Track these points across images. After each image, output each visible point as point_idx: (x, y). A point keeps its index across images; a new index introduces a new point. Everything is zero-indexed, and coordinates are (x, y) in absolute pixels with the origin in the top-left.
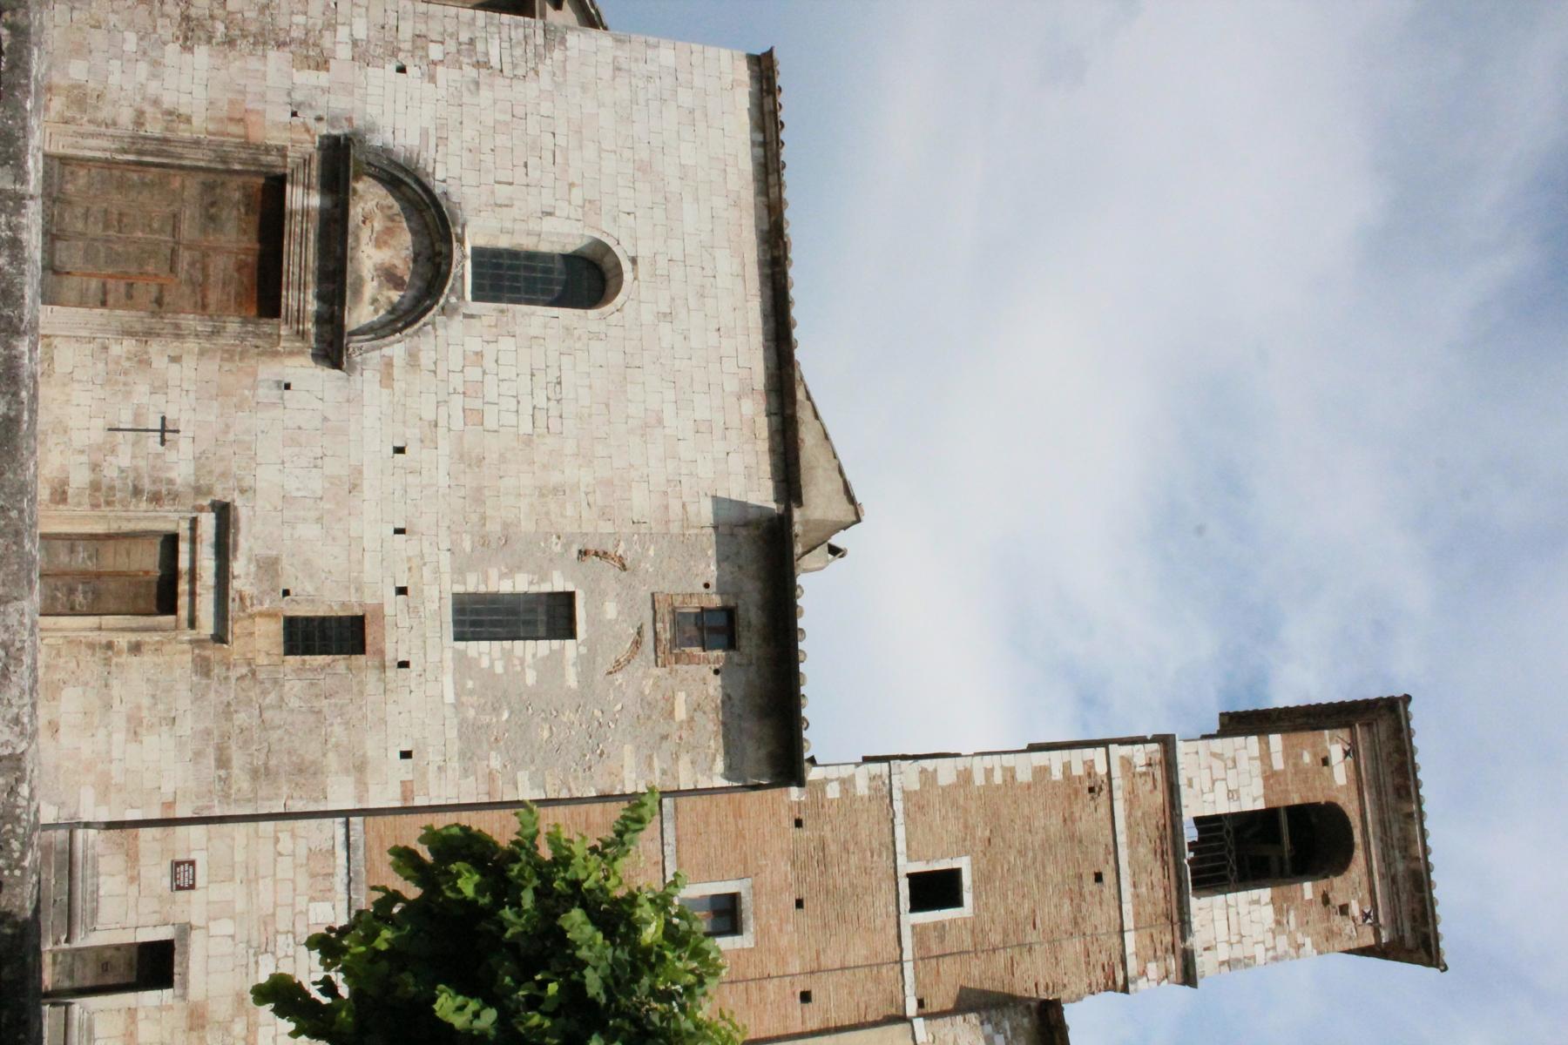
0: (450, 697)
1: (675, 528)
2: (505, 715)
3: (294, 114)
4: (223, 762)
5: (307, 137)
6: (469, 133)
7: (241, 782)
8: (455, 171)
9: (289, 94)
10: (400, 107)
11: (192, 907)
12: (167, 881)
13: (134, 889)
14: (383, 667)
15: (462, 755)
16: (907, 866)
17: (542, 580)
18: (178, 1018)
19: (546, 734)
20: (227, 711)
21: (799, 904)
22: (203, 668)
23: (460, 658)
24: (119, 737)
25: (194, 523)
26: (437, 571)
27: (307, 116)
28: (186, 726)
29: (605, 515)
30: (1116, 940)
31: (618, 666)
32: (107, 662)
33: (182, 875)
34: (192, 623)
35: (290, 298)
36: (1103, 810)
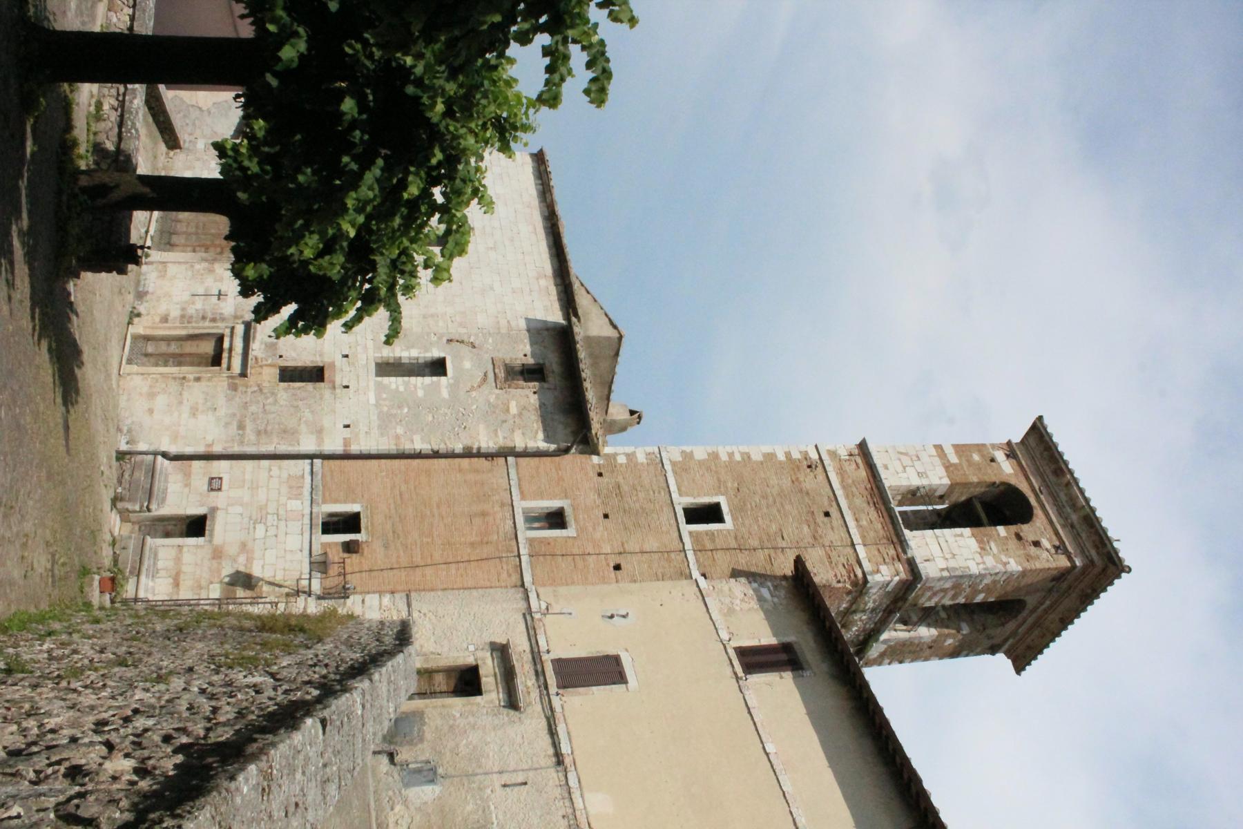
0: (372, 401)
1: (504, 331)
2: (406, 410)
4: (241, 427)
7: (250, 435)
11: (219, 499)
12: (206, 487)
13: (186, 490)
14: (334, 388)
15: (380, 427)
17: (427, 351)
18: (206, 552)
19: (430, 418)
20: (246, 405)
22: (234, 388)
23: (378, 385)
24: (185, 415)
25: (233, 328)
26: (365, 347)
29: (461, 325)
30: (849, 550)
32: (182, 385)
33: (215, 485)
34: (229, 368)
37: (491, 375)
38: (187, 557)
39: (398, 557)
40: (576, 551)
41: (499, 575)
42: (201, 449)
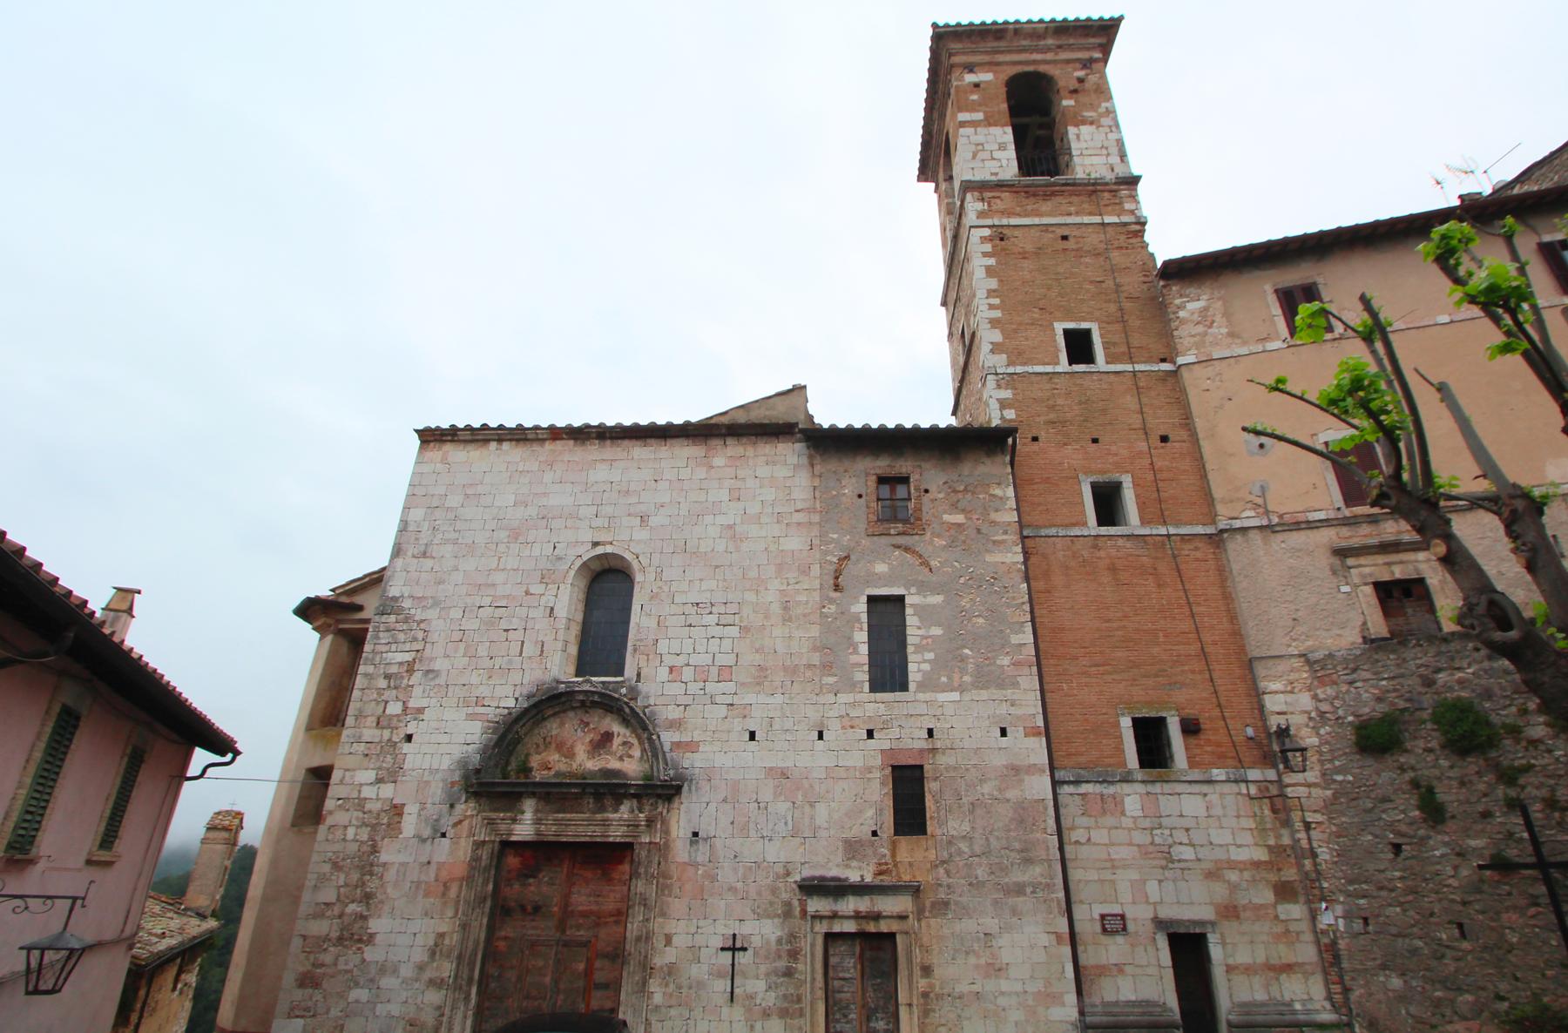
0: (955, 696)
1: (816, 518)
2: (967, 651)
3: (444, 835)
4: (1019, 890)
5: (466, 823)
6: (475, 679)
8: (509, 690)
9: (424, 841)
10: (445, 738)
11: (1138, 915)
12: (1120, 939)
13: (1128, 969)
15: (1001, 686)
16: (1063, 365)
17: (859, 620)
18: (1230, 928)
19: (981, 620)
20: (976, 885)
21: (1095, 441)
22: (942, 906)
23: (922, 686)
24: (1004, 985)
25: (817, 917)
26: (853, 704)
27: (446, 823)
28: (991, 923)
30: (1109, 229)
31: (925, 564)
32: (939, 997)
33: (1114, 925)
34: (902, 917)
35: (616, 834)
36: (1016, 233)
38: (1242, 957)
39: (1193, 672)
40: (1150, 477)
41: (1197, 560)
42: (1067, 950)
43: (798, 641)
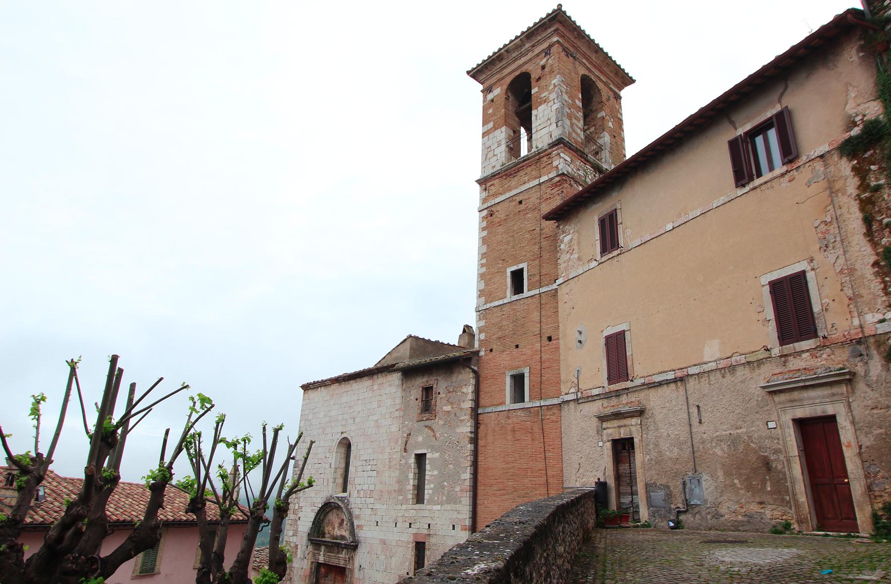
0: (439, 507)
1: (402, 413)
14: (429, 535)
15: (455, 503)
29: (396, 443)
30: (543, 186)
31: (434, 436)
37: (428, 423)
39: (540, 495)
41: (553, 421)
43: (390, 478)
